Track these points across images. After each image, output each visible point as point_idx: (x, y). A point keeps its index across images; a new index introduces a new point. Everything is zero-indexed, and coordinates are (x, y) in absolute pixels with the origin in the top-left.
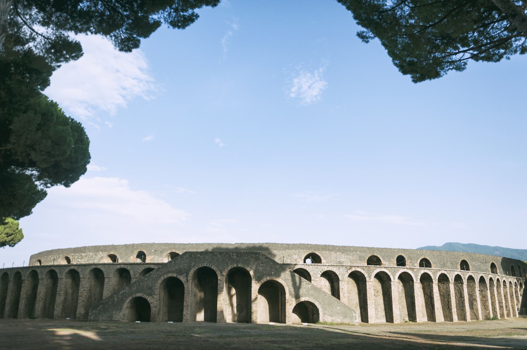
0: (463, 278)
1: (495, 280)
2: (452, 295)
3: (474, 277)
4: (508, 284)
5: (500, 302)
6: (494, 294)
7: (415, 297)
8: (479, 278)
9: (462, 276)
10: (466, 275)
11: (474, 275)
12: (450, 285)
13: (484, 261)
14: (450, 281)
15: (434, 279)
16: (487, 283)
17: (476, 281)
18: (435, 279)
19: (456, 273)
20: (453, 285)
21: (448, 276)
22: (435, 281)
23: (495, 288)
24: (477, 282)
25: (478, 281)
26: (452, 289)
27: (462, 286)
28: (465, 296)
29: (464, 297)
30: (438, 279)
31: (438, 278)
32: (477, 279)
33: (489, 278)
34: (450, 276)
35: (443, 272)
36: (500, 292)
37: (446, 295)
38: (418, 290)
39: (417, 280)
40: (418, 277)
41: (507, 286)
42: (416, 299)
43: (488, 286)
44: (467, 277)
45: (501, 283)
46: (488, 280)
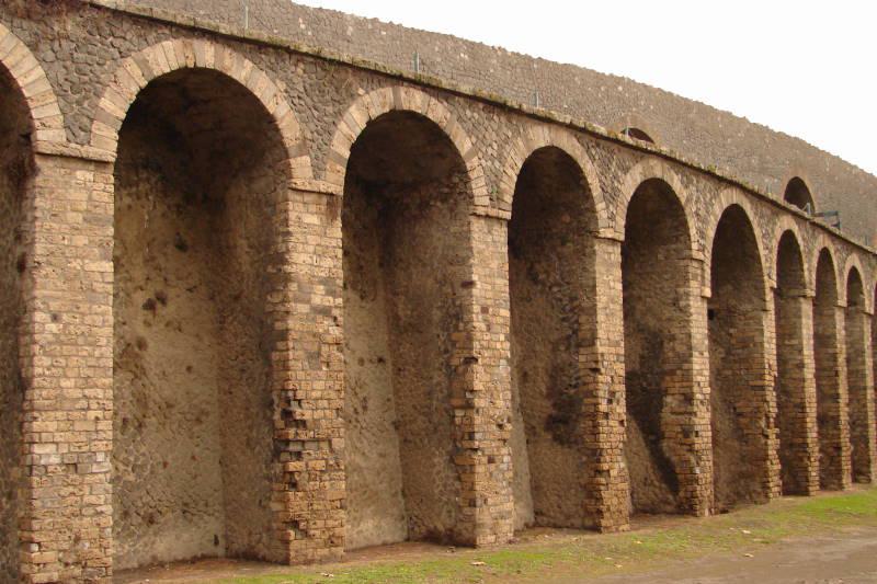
0: (596, 192)
1: (810, 252)
2: (485, 310)
3: (683, 201)
4: (869, 292)
5: (827, 395)
6: (794, 342)
7: (39, 316)
8: (718, 211)
9: (590, 170)
10: (626, 170)
11: (686, 187)
12: (477, 226)
13: (755, 161)
14: (479, 188)
15: (303, 148)
16: (765, 264)
17: (693, 232)
18: (317, 146)
19: (541, 137)
20: (501, 234)
21: (464, 144)
22: (318, 171)
23: (807, 308)
24: (702, 235)
25: (711, 233)
26: (494, 265)
27: (585, 255)
28: (601, 334)
29: (593, 339)
30: (347, 154)
31: (353, 148)
32: (704, 221)
33: (779, 234)
34: (475, 151)
35: (416, 101)
36: (829, 337)
37: (437, 315)
38: (81, 240)
39: (77, 126)
40: (105, 103)
41: (867, 302)
42: (43, 326)
43: (771, 281)
44: (629, 184)
45: (838, 281)
46: (775, 244)
